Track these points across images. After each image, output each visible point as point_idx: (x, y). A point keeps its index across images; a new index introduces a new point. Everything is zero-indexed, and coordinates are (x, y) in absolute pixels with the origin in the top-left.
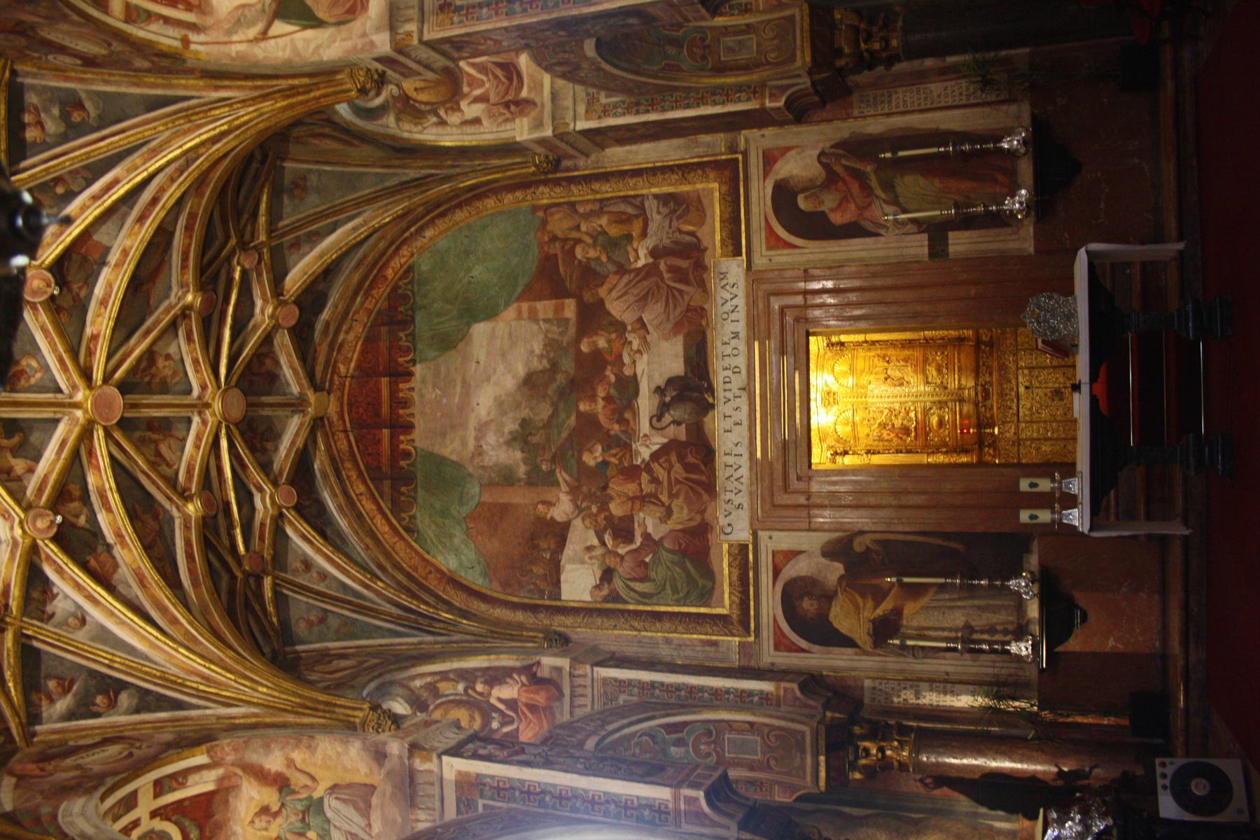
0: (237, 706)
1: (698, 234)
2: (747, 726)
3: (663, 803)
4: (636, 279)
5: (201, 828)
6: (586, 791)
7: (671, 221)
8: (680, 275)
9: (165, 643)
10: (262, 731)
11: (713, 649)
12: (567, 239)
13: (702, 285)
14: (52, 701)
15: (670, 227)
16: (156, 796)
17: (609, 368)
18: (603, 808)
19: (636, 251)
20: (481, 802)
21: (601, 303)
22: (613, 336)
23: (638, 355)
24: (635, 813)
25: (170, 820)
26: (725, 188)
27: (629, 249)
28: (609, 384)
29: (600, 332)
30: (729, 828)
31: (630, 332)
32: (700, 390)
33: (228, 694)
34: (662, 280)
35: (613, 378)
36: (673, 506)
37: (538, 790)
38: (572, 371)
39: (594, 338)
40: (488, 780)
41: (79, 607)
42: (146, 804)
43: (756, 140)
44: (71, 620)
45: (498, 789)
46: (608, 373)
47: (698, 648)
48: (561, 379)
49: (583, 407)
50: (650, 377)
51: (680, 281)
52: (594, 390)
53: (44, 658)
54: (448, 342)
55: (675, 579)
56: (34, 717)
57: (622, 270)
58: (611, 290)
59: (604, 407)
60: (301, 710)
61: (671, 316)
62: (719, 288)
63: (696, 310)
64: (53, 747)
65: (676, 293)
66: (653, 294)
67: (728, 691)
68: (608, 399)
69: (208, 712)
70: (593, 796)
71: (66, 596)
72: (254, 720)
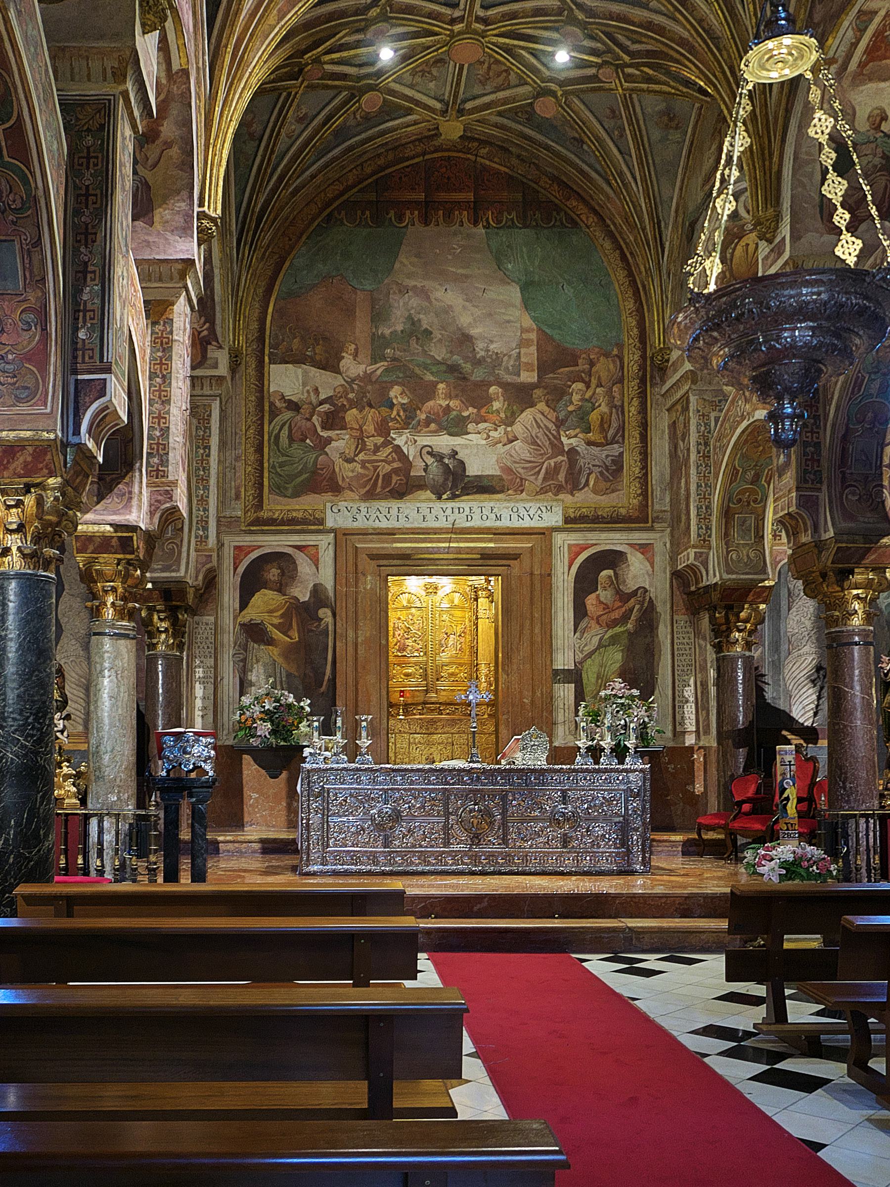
1: (586, 489)
2: (180, 526)
4: (551, 437)
7: (599, 466)
8: (551, 474)
11: (233, 496)
12: (590, 376)
13: (543, 491)
15: (594, 466)
17: (475, 411)
18: (156, 426)
19: (576, 436)
21: (532, 405)
22: (503, 415)
23: (485, 436)
26: (623, 511)
27: (578, 430)
28: (460, 411)
29: (506, 403)
31: (505, 429)
32: (454, 486)
34: (549, 458)
35: (465, 414)
36: (355, 464)
38: (473, 378)
39: (501, 398)
43: (660, 540)
46: (470, 409)
47: (233, 483)
48: (467, 367)
49: (441, 386)
50: (466, 446)
51: (546, 473)
52: (457, 396)
54: (499, 259)
55: (292, 464)
57: (560, 423)
58: (543, 414)
59: (441, 406)
61: (517, 465)
62: (538, 505)
63: (521, 485)
65: (537, 469)
66: (536, 450)
67: (206, 510)
68: (448, 409)
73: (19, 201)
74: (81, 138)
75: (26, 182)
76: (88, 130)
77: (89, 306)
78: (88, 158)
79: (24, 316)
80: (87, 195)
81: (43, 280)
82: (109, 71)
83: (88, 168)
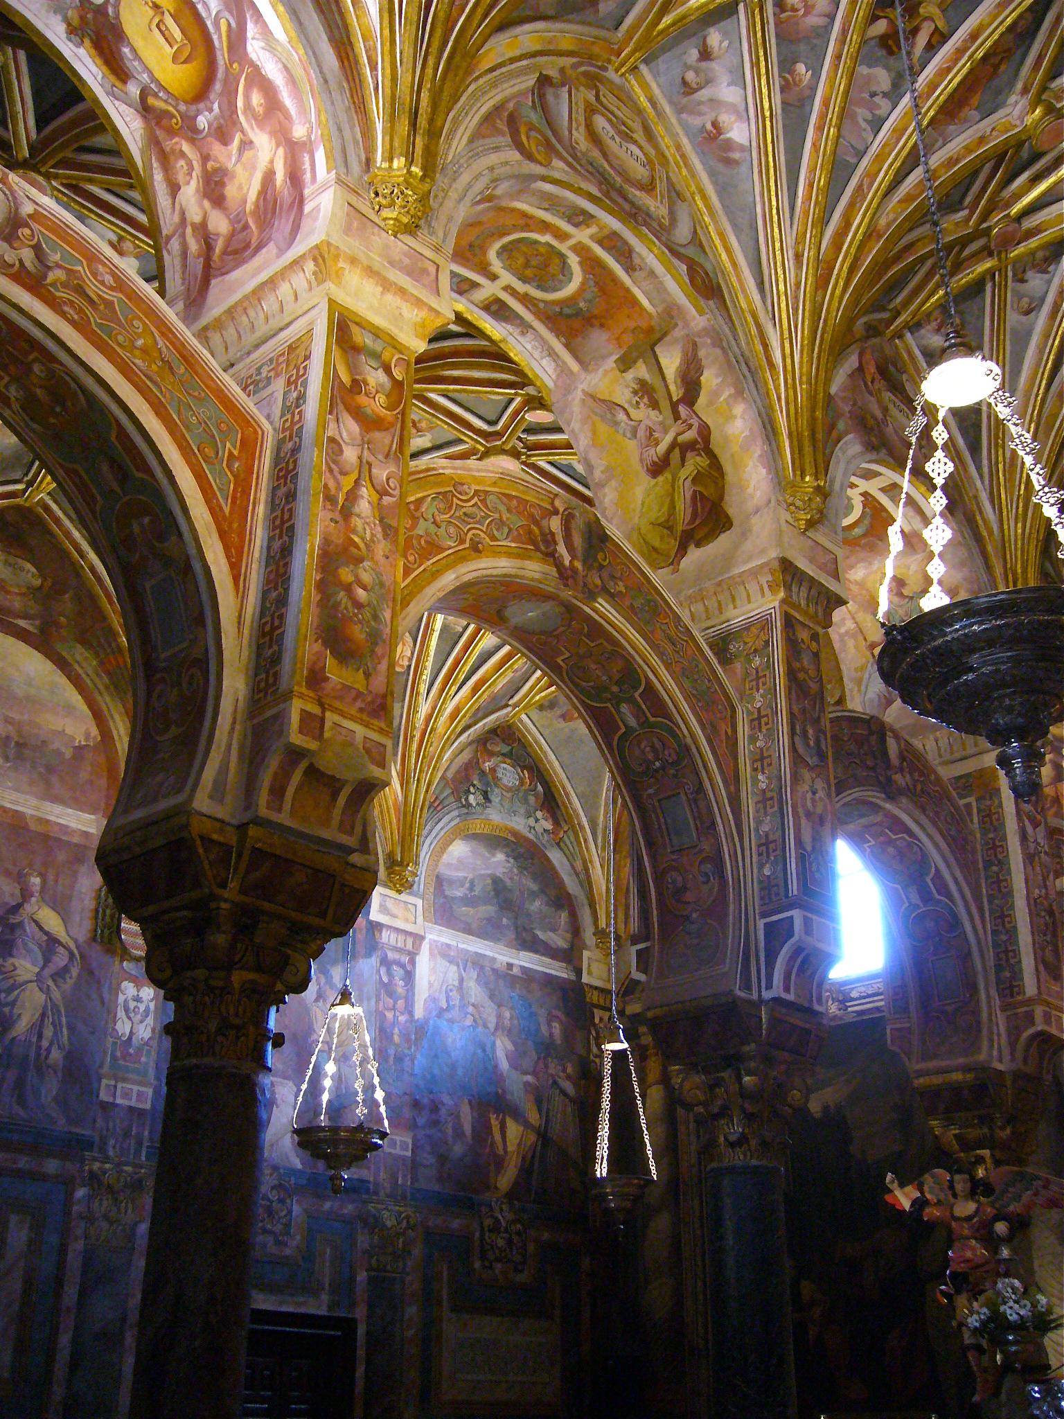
0: (994, 508)
3: (1021, 991)
5: (865, 535)
6: (1012, 907)
9: (1034, 406)
10: (976, 550)
14: (938, 330)
16: (882, 490)
18: (1000, 928)
20: (972, 800)
24: (1003, 963)
25: (864, 507)
30: (1013, 1059)
33: (1003, 496)
37: (1000, 857)
40: (997, 802)
41: (1042, 300)
42: (873, 487)
44: (1026, 300)
45: (989, 815)
53: (978, 299)
56: (915, 327)
60: (1010, 576)
64: (895, 366)
69: (978, 483)
70: (1009, 915)
71: (1049, 282)
72: (985, 533)
73: (673, 754)
74: (749, 661)
75: (674, 735)
76: (756, 651)
77: (771, 837)
78: (758, 678)
79: (703, 868)
80: (759, 718)
81: (713, 825)
82: (765, 586)
83: (758, 691)
